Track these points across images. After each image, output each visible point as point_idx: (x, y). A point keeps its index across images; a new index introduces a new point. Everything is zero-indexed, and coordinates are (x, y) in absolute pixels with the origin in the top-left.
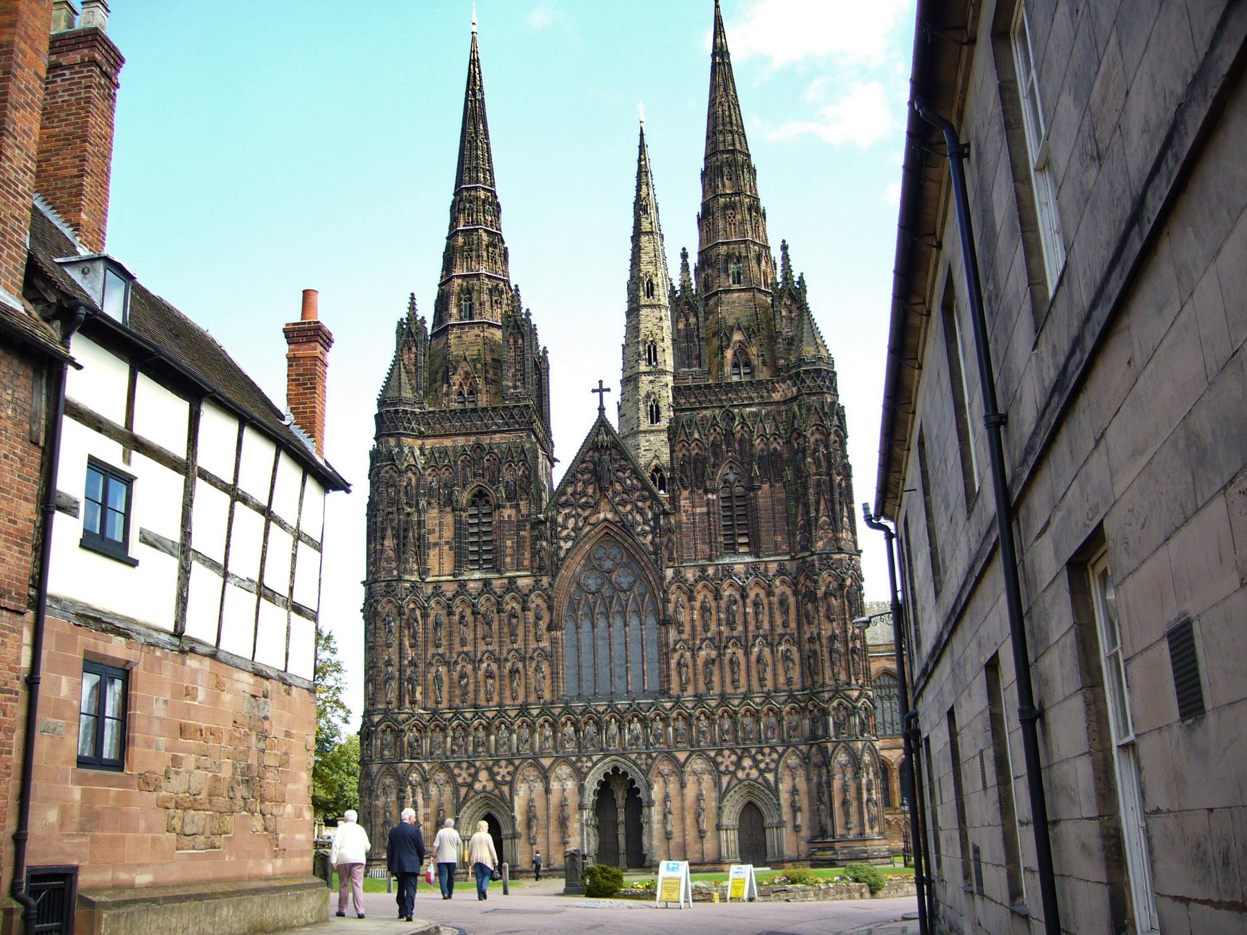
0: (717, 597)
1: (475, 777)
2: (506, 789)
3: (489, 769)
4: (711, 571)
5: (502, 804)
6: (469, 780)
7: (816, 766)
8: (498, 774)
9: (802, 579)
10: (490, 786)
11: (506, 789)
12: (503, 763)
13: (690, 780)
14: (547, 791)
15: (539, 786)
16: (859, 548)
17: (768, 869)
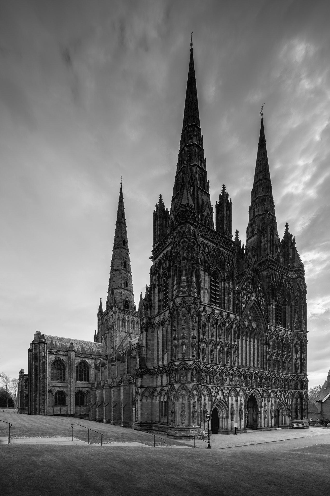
0: (278, 339)
1: (217, 393)
2: (226, 399)
3: (222, 390)
4: (277, 330)
5: (225, 405)
6: (216, 394)
7: (296, 398)
8: (225, 392)
9: (295, 338)
10: (222, 397)
11: (226, 399)
12: (226, 389)
13: (270, 399)
14: (237, 401)
15: (234, 399)
16: (307, 330)
17: (281, 429)
